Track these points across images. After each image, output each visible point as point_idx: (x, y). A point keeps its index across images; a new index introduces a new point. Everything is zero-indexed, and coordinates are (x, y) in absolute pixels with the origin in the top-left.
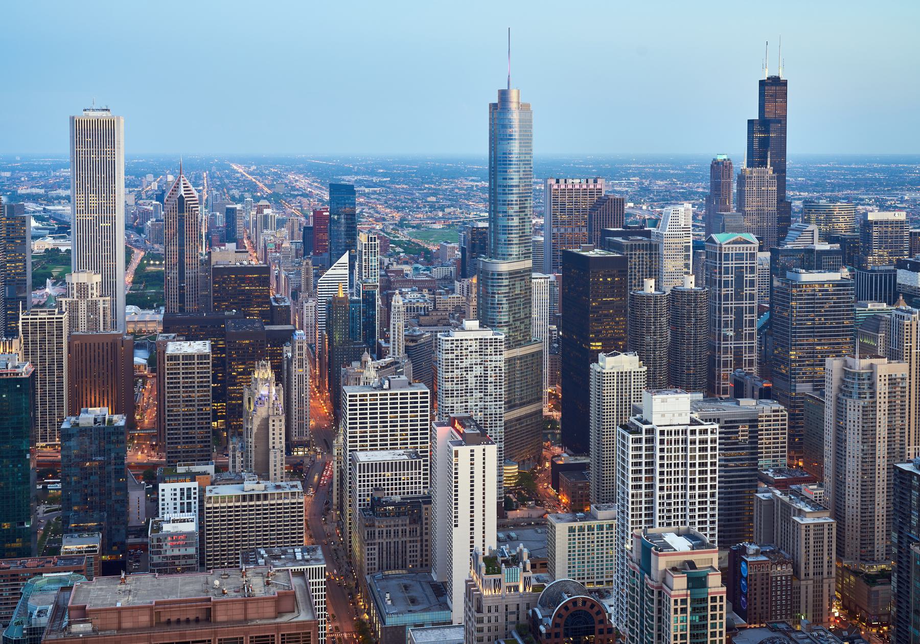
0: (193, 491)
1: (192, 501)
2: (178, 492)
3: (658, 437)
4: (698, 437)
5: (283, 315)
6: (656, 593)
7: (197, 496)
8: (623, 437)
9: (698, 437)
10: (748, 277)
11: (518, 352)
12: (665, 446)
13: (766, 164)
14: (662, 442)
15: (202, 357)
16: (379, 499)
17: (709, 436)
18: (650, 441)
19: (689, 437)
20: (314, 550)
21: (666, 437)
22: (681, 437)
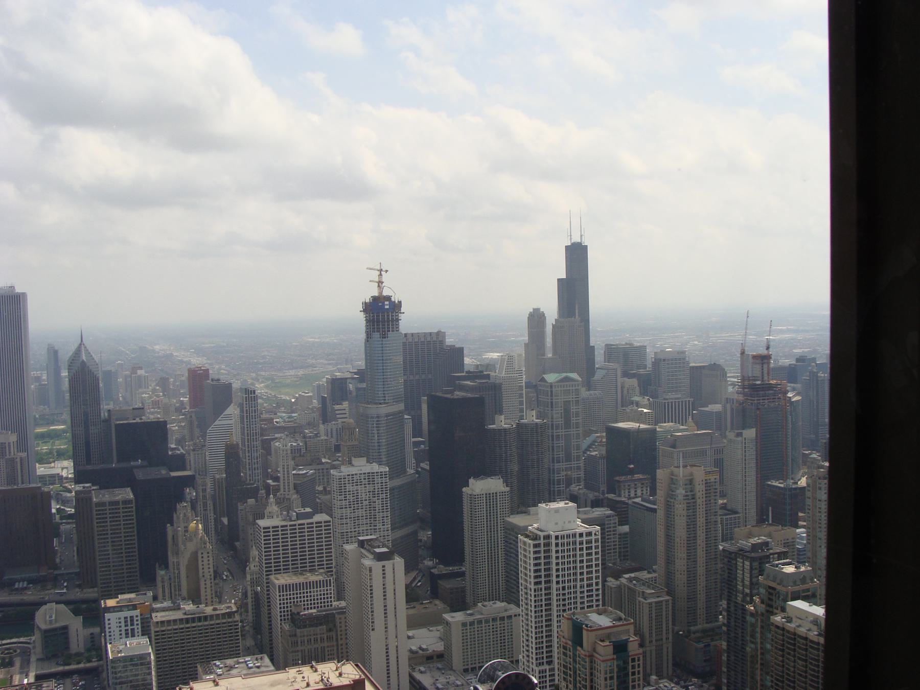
0: (135, 619)
1: (135, 627)
2: (123, 620)
3: (553, 541)
4: (584, 538)
5: (180, 462)
6: (587, 660)
7: (139, 622)
8: (525, 543)
9: (584, 538)
10: (573, 408)
11: (397, 482)
12: (560, 548)
13: (575, 314)
14: (557, 545)
15: (130, 502)
16: (298, 613)
17: (593, 537)
18: (547, 545)
19: (578, 539)
20: (261, 659)
21: (560, 541)
22: (571, 540)
